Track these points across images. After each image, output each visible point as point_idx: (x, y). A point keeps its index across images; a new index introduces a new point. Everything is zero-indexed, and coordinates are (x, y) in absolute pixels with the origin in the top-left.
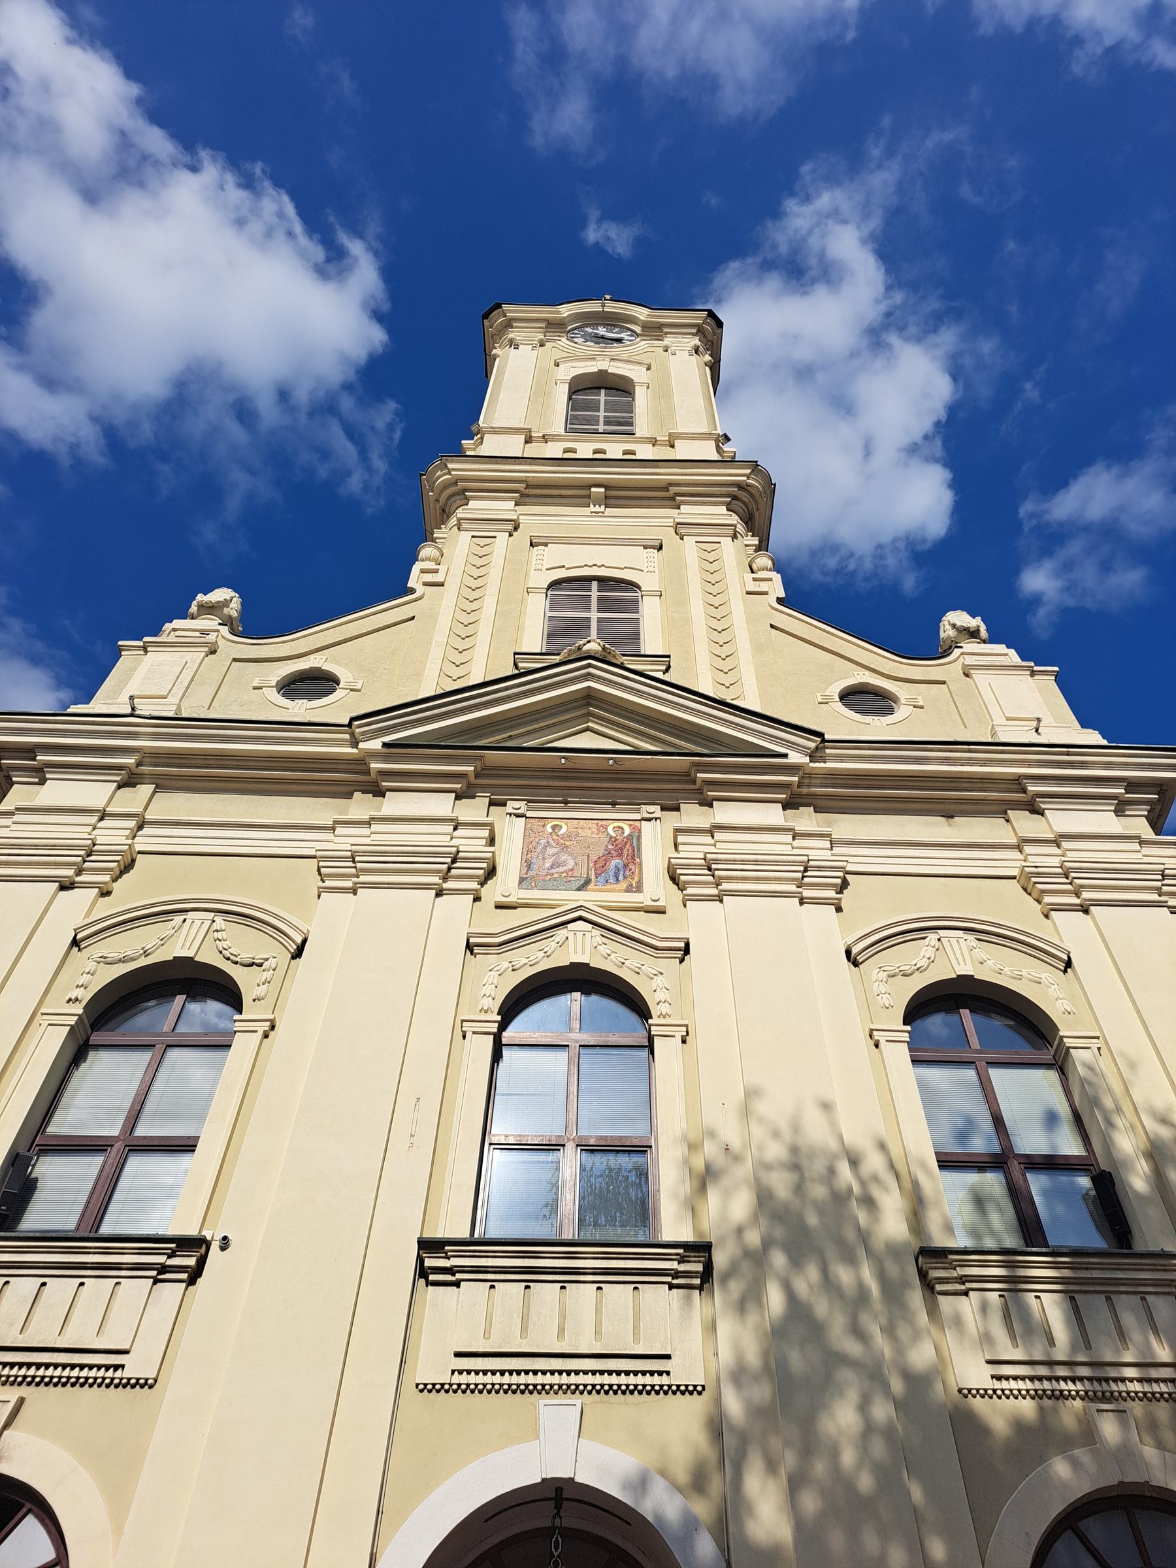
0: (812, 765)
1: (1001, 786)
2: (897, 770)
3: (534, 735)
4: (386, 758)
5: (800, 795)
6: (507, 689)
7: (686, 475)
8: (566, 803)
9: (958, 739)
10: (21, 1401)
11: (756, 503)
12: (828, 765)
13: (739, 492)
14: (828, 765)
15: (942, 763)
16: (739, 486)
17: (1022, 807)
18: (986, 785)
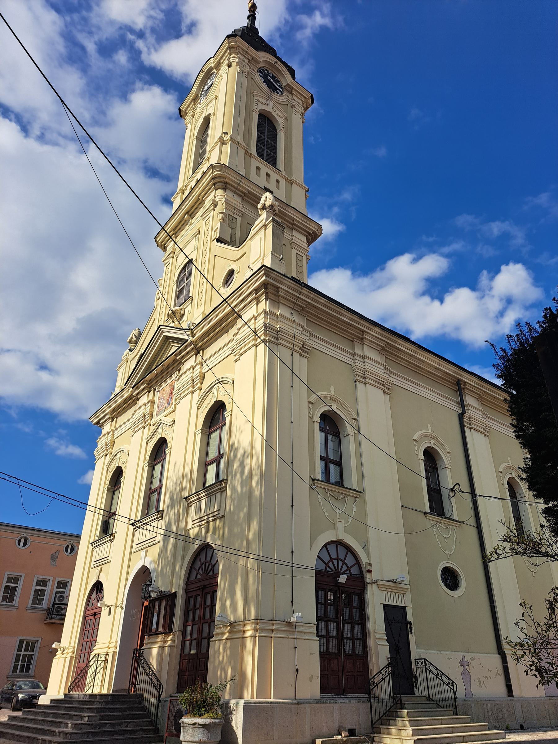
0: (194, 339)
1: (232, 314)
4: (134, 391)
5: (198, 348)
6: (148, 352)
7: (200, 189)
9: (216, 306)
10: (102, 568)
11: (223, 177)
12: (197, 336)
14: (197, 336)
15: (216, 317)
16: (213, 179)
18: (228, 316)
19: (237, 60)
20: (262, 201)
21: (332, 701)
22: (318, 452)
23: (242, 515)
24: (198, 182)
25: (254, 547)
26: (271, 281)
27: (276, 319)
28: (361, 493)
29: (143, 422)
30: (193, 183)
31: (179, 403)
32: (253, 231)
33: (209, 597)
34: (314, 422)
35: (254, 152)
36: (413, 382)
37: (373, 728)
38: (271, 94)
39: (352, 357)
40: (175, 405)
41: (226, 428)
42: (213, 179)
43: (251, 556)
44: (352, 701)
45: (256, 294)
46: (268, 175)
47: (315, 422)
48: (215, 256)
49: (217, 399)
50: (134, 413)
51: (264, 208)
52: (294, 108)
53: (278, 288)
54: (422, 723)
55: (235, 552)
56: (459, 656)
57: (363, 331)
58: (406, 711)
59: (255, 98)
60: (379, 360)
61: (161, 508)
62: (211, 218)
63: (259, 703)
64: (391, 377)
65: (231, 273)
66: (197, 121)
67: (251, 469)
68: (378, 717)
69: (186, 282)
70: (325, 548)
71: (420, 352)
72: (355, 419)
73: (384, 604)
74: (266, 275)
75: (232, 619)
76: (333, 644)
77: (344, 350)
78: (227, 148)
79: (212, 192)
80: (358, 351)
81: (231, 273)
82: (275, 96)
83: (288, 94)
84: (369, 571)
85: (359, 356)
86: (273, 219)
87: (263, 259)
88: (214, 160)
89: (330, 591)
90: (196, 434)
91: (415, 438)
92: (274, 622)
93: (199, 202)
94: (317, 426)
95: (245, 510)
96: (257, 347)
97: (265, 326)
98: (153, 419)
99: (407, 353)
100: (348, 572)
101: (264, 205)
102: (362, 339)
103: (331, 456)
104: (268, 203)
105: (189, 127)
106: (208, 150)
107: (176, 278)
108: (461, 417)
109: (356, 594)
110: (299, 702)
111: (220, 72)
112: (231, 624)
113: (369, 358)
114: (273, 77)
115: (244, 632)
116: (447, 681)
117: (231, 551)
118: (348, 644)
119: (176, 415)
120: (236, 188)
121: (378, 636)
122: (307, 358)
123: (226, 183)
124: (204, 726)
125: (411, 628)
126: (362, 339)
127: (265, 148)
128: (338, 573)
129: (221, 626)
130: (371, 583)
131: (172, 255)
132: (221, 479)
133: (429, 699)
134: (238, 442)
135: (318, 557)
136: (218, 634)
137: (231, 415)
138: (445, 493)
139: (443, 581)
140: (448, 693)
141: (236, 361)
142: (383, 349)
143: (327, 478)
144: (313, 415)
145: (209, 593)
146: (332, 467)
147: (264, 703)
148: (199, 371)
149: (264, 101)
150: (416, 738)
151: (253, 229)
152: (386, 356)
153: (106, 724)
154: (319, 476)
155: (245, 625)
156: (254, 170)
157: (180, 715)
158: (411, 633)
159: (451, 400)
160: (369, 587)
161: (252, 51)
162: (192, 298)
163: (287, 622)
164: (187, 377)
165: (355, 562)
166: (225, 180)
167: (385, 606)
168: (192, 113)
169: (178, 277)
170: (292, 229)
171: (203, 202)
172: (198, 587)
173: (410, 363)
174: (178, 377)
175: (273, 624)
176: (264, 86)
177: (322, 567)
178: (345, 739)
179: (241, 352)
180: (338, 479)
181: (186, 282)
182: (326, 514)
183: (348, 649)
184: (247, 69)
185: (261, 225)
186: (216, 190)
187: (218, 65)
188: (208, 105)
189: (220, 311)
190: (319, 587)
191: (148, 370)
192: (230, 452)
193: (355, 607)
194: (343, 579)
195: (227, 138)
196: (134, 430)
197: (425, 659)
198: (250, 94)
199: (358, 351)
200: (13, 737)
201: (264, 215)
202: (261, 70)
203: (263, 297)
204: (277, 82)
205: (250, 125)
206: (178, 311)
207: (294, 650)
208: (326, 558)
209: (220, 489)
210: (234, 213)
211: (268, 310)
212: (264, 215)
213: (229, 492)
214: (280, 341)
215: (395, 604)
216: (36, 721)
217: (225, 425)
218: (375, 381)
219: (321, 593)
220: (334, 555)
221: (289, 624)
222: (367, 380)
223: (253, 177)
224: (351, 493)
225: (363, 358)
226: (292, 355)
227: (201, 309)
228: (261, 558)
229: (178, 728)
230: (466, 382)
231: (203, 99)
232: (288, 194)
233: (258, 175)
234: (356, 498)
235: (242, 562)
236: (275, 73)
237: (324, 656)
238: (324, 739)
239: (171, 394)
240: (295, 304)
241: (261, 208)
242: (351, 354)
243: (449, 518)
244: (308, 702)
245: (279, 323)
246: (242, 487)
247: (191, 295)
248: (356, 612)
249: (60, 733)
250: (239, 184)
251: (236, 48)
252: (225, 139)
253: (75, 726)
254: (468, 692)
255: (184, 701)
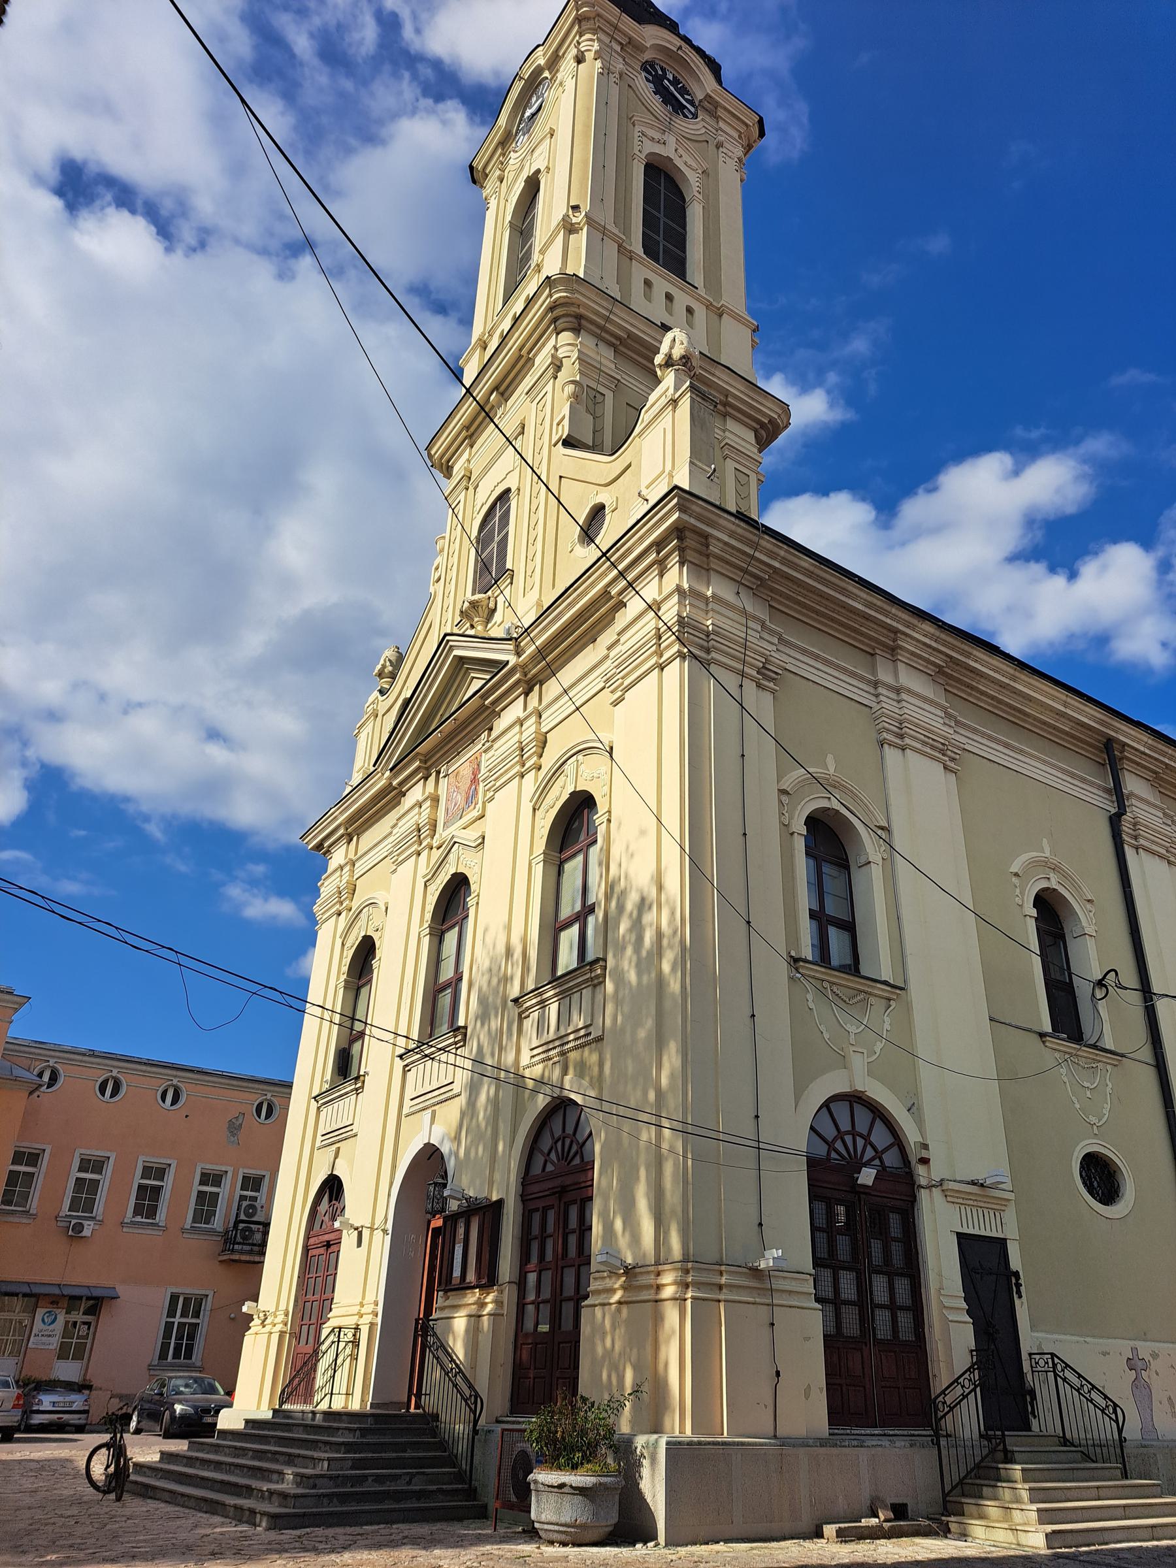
0: (521, 659)
1: (603, 601)
2: (553, 633)
3: (452, 703)
4: (395, 776)
5: (531, 679)
6: (421, 692)
7: (522, 333)
8: (473, 742)
9: (568, 586)
10: (339, 1148)
12: (528, 652)
13: (554, 313)
14: (528, 652)
16: (551, 309)
17: (619, 608)
18: (597, 606)
19: (596, 46)
20: (664, 348)
21: (855, 1443)
22: (804, 901)
23: (642, 1034)
24: (516, 320)
25: (673, 1103)
26: (692, 521)
27: (702, 605)
28: (901, 989)
29: (415, 841)
30: (506, 325)
31: (492, 799)
32: (645, 417)
33: (574, 1212)
34: (792, 834)
35: (638, 248)
36: (1007, 745)
37: (945, 1502)
38: (670, 119)
39: (872, 690)
40: (484, 803)
41: (594, 851)
42: (551, 308)
43: (665, 1123)
44: (898, 1444)
45: (658, 553)
46: (669, 297)
47: (796, 834)
48: (561, 477)
49: (575, 787)
50: (397, 824)
51: (669, 363)
52: (721, 149)
53: (706, 537)
54: (1059, 1494)
55: (629, 1113)
56: (1124, 1347)
57: (896, 631)
58: (1018, 1467)
59: (637, 128)
60: (932, 696)
61: (461, 1023)
62: (549, 396)
63: (700, 1443)
64: (958, 733)
65: (598, 511)
66: (509, 189)
67: (659, 935)
68: (956, 1479)
69: (497, 539)
70: (824, 1109)
71: (1024, 676)
72: (882, 828)
73: (958, 1234)
74: (681, 507)
75: (630, 1260)
76: (850, 1316)
77: (853, 675)
78: (580, 240)
79: (548, 339)
80: (885, 676)
81: (598, 511)
82: (680, 123)
83: (708, 119)
84: (925, 1161)
85: (890, 688)
86: (692, 386)
87: (671, 476)
88: (552, 266)
89: (840, 1202)
90: (533, 865)
91: (1014, 869)
92: (723, 1268)
93: (522, 363)
94: (800, 845)
95: (650, 1023)
96: (662, 669)
97: (681, 621)
98: (437, 836)
99: (994, 681)
100: (877, 1162)
101: (669, 356)
102: (893, 650)
103: (830, 909)
104: (677, 353)
105: (493, 203)
106: (537, 248)
107: (474, 533)
108: (1115, 822)
109: (894, 1210)
110: (785, 1442)
111: (559, 75)
112: (629, 1271)
113: (909, 691)
114: (675, 82)
115: (659, 1288)
116: (1103, 1403)
117: (622, 1111)
118: (882, 1318)
119: (488, 826)
120: (603, 328)
121: (947, 1302)
122: (773, 692)
123: (579, 317)
124: (581, 1491)
125: (1018, 1285)
126: (893, 650)
127: (661, 239)
128: (858, 1166)
129: (605, 1274)
130: (929, 1187)
131: (464, 483)
132: (590, 956)
133: (1065, 1441)
134: (626, 877)
135: (812, 1128)
136: (598, 1292)
137: (609, 821)
138: (1083, 990)
139: (1084, 1183)
140: (1105, 1429)
141: (615, 703)
142: (940, 671)
143: (823, 956)
144: (791, 818)
145: (574, 1202)
146: (833, 932)
147: (709, 1443)
148: (533, 729)
149: (657, 136)
150: (1050, 1528)
151: (647, 412)
152: (947, 687)
153: (366, 1477)
154: (807, 952)
155: (658, 1274)
156: (638, 287)
157: (525, 1465)
158: (1020, 1297)
159: (1092, 784)
160: (923, 1195)
161: (628, 24)
162: (511, 573)
163: (750, 1269)
164: (506, 745)
165: (890, 1140)
166: (576, 310)
167: (960, 1236)
168: (498, 173)
169: (480, 531)
170: (725, 415)
171: (530, 362)
172: (549, 1189)
173: (1000, 701)
174: (487, 745)
175: (721, 1274)
176: (656, 102)
177: (821, 1150)
178: (886, 1525)
179: (627, 682)
180: (848, 961)
181: (497, 539)
182: (826, 1036)
183: (883, 1328)
184: (620, 66)
185: (663, 401)
186: (558, 334)
187: (554, 61)
188: (532, 151)
189: (578, 595)
190: (816, 1194)
191: (423, 732)
192: (608, 898)
193: (895, 1240)
194: (867, 1177)
195: (578, 218)
196: (397, 860)
197: (1053, 1355)
198: (627, 120)
199: (885, 676)
200: (174, 1498)
201: (669, 379)
202: (648, 67)
203: (675, 558)
204: (684, 91)
205: (628, 190)
206: (482, 603)
207: (768, 1330)
208: (829, 1132)
209: (592, 979)
210: (598, 382)
211: (686, 586)
212: (669, 379)
213: (609, 986)
214: (713, 655)
215: (983, 1233)
216: (218, 1466)
217: (595, 841)
218: (925, 743)
219: (821, 1207)
220: (845, 1126)
221: (756, 1272)
222: (907, 741)
223: (638, 301)
224: (879, 989)
225: (898, 690)
226: (741, 686)
227: (533, 596)
228: (690, 1129)
229: (523, 1492)
230: (1124, 744)
231: (522, 139)
232: (714, 336)
233: (648, 297)
234: (889, 1000)
235: (647, 1135)
236: (678, 73)
237: (830, 1342)
238: (842, 1525)
239: (475, 780)
240: (746, 571)
241: (663, 363)
242: (869, 682)
243: (1090, 1046)
244: (803, 1443)
245: (711, 614)
246: (639, 974)
247: (509, 566)
248: (896, 1249)
249: (271, 1493)
250: (607, 319)
251: (594, 18)
252: (574, 220)
253: (301, 1479)
254: (1148, 1427)
255: (535, 1435)
